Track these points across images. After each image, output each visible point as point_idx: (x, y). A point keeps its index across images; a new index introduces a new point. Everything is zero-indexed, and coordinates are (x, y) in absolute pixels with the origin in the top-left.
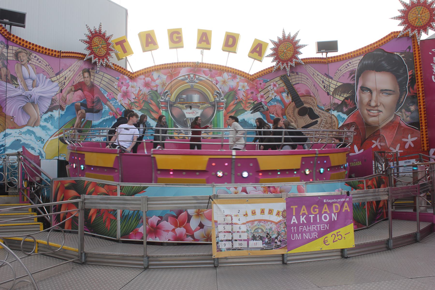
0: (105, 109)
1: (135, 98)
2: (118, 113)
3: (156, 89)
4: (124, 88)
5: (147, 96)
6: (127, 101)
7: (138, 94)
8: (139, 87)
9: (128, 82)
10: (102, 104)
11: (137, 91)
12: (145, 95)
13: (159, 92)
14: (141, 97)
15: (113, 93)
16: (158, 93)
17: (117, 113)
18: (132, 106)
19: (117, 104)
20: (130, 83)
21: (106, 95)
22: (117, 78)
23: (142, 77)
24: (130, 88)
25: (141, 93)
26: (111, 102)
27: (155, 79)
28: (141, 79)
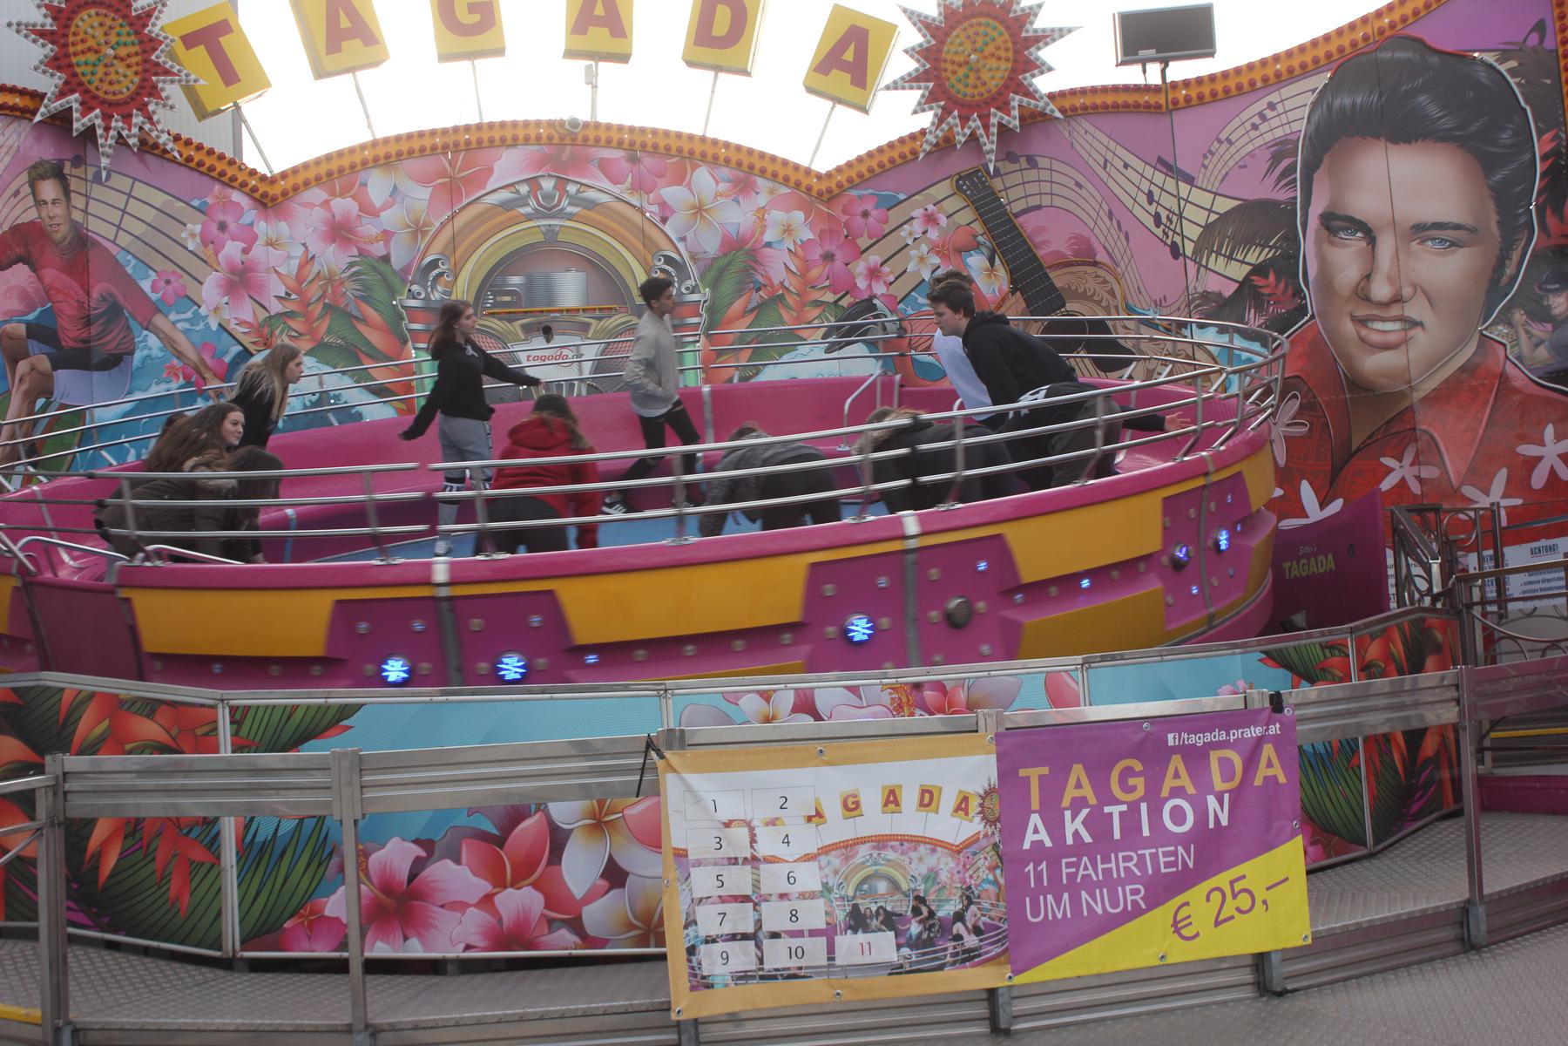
0: (146, 352)
1: (287, 293)
2: (209, 369)
3: (383, 252)
4: (232, 250)
5: (342, 283)
6: (247, 311)
7: (299, 278)
8: (304, 245)
9: (252, 224)
10: (129, 329)
11: (295, 263)
12: (330, 279)
13: (397, 262)
14: (314, 292)
15: (181, 277)
16: (394, 272)
17: (203, 369)
18: (272, 333)
19: (201, 326)
20: (261, 227)
21: (146, 285)
22: (196, 203)
23: (317, 194)
24: (258, 251)
25: (315, 269)
26: (173, 317)
27: (378, 203)
28: (311, 205)
